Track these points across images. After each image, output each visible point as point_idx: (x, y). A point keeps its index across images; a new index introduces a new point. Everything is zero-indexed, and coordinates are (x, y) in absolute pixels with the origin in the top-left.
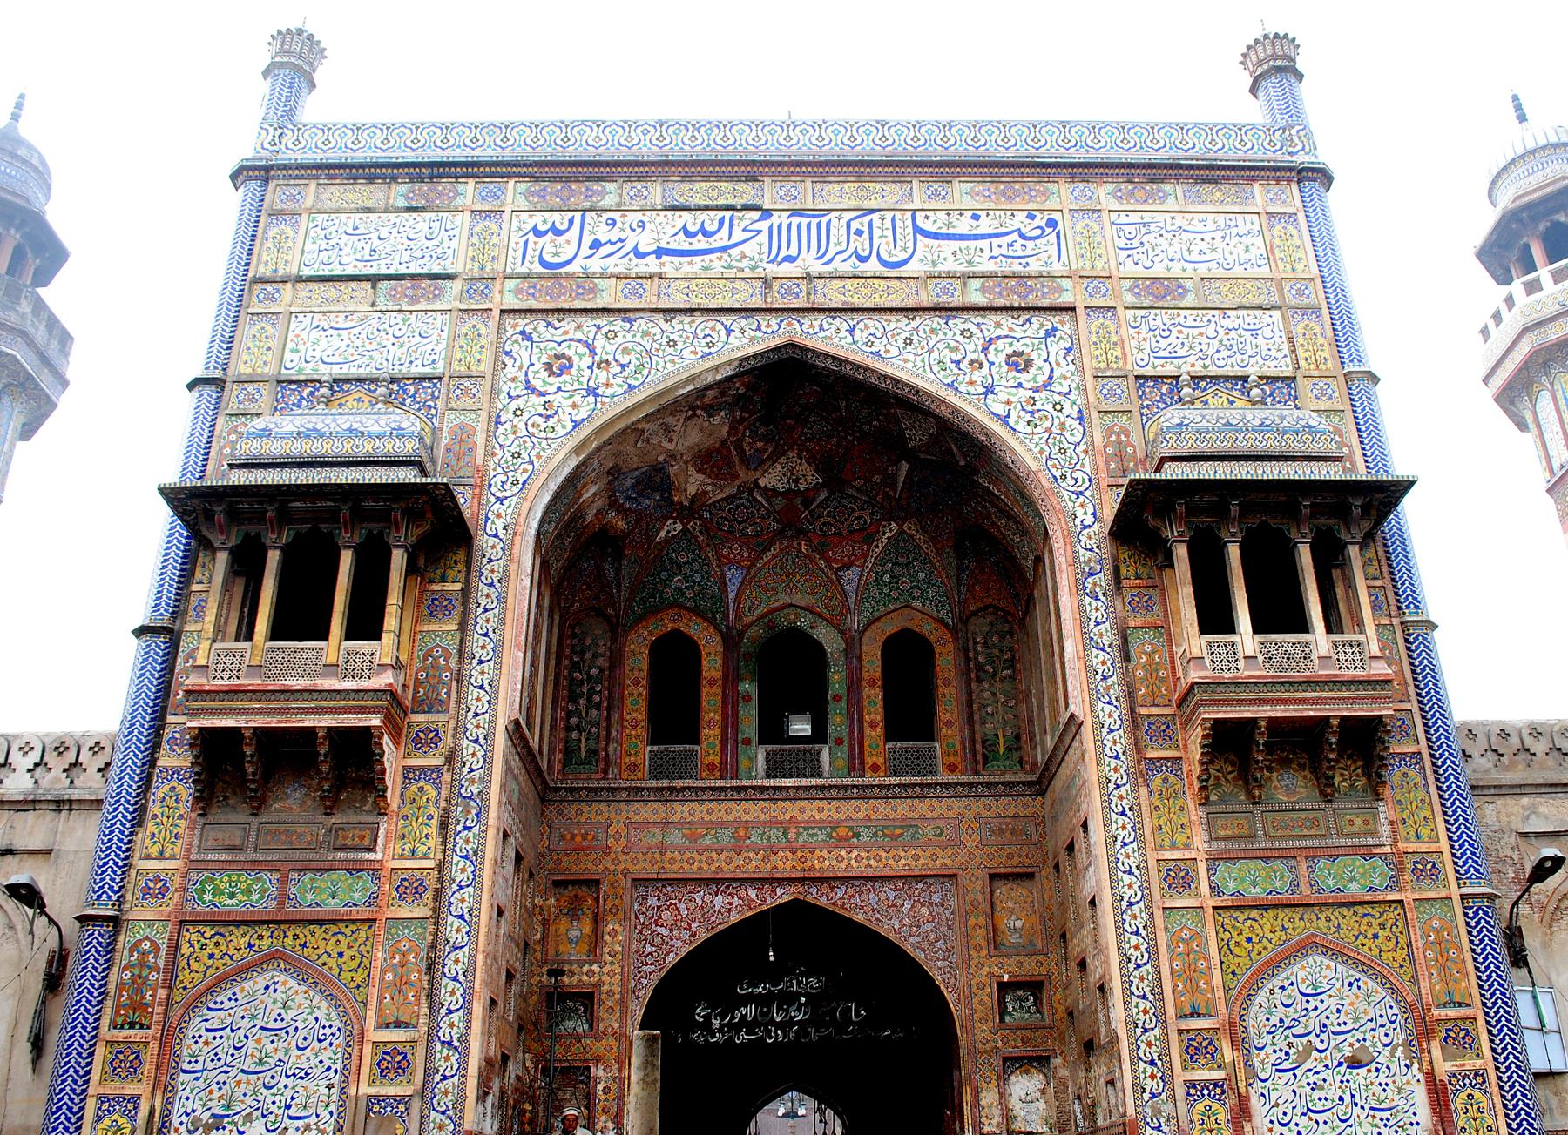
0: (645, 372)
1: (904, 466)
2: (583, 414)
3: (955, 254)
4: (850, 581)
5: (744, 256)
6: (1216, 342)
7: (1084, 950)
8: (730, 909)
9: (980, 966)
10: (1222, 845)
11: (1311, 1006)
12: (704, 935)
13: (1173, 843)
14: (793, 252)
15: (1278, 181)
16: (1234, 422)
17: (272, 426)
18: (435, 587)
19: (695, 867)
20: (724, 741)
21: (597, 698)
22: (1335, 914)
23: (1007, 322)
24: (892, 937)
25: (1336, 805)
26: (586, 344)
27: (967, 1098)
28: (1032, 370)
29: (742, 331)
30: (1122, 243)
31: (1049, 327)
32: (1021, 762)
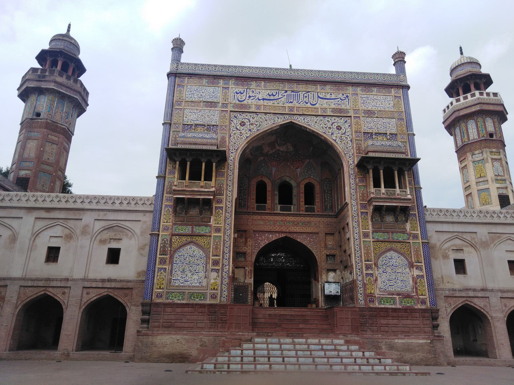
0: (261, 126)
1: (312, 148)
2: (248, 135)
3: (326, 103)
4: (298, 171)
5: (281, 101)
6: (381, 125)
7: (346, 248)
8: (273, 237)
9: (323, 251)
10: (375, 229)
11: (390, 261)
12: (267, 242)
13: (365, 228)
14: (292, 101)
15: (397, 88)
16: (384, 144)
17: (185, 135)
18: (219, 170)
19: (266, 229)
20: (272, 203)
21: (245, 193)
22: (396, 244)
23: (337, 119)
24: (305, 244)
25: (398, 223)
26: (248, 119)
27: (320, 277)
28: (342, 130)
29: (281, 118)
30: (362, 102)
31: (346, 120)
32: (332, 211)
